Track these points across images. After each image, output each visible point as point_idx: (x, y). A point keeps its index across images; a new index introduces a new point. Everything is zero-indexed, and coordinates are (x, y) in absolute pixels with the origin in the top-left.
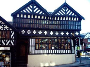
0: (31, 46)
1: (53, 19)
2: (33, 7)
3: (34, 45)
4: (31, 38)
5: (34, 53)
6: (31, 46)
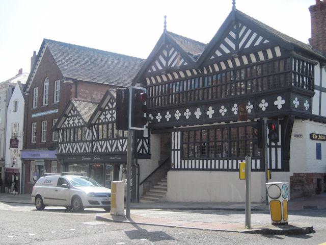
2: (168, 53)
4: (175, 131)
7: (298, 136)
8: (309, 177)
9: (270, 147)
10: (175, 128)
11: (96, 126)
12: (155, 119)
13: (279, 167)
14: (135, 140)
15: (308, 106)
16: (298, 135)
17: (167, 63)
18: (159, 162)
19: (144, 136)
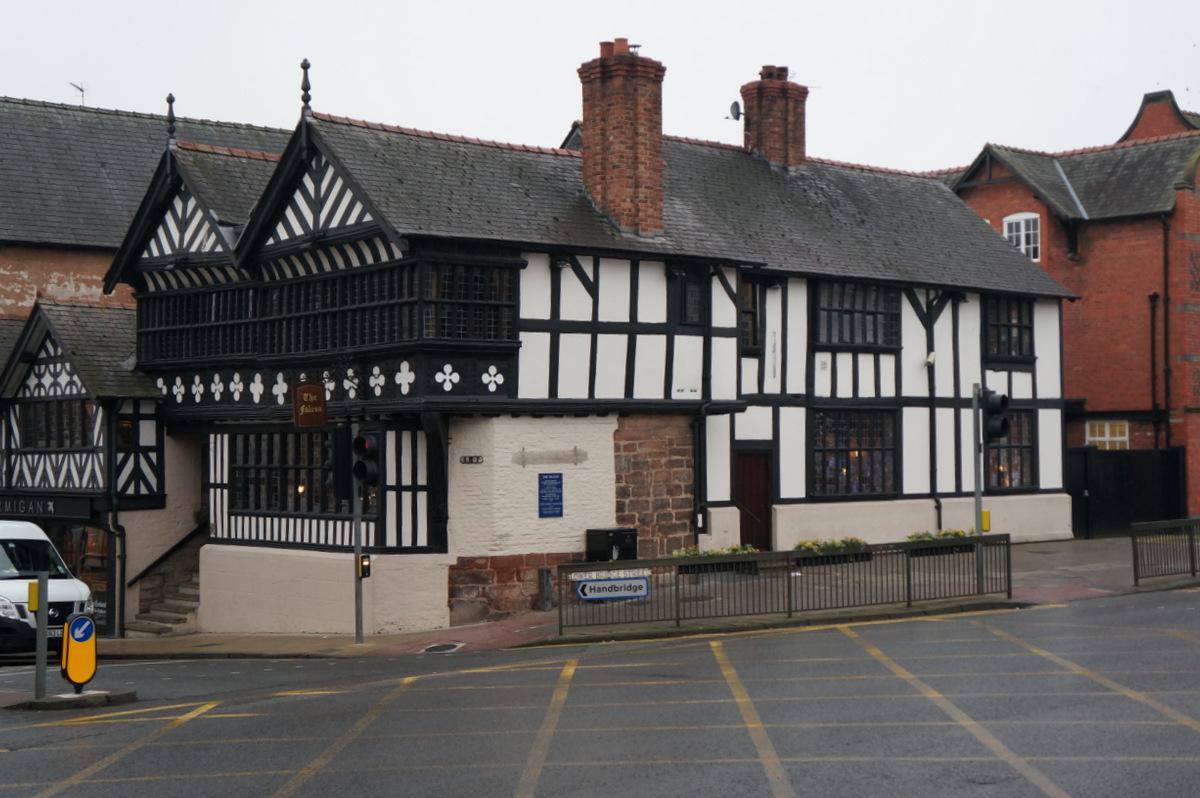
7: (469, 460)
8: (507, 568)
9: (399, 489)
10: (217, 423)
12: (171, 396)
13: (422, 541)
14: (110, 459)
15: (500, 379)
16: (471, 458)
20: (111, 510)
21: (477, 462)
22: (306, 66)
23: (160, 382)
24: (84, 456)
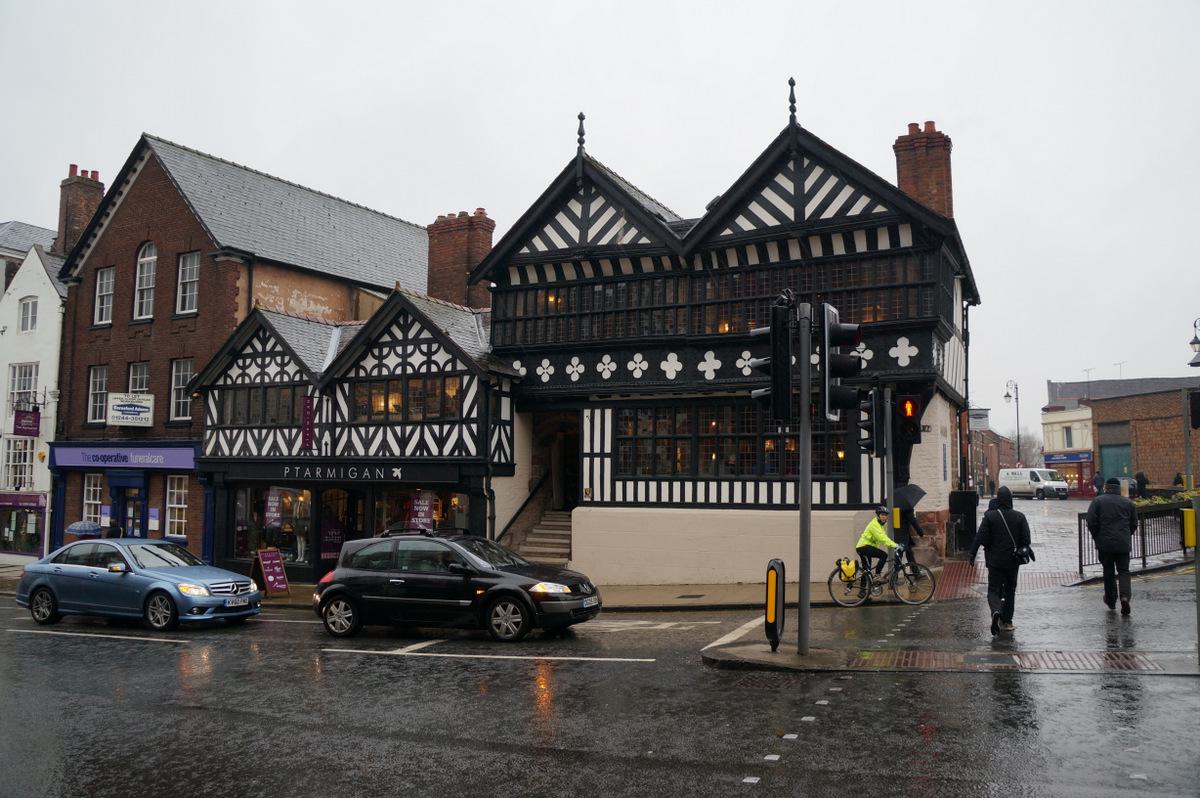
0: (592, 455)
1: (716, 266)
2: (586, 210)
3: (608, 449)
5: (607, 498)
6: (592, 455)
11: (346, 386)
12: (532, 377)
17: (584, 234)
18: (530, 482)
19: (503, 418)
20: (487, 475)
21: (928, 431)
22: (792, 83)
23: (517, 365)
24: (446, 428)
